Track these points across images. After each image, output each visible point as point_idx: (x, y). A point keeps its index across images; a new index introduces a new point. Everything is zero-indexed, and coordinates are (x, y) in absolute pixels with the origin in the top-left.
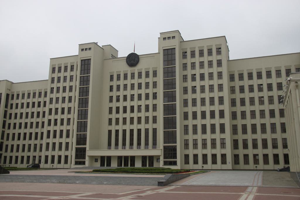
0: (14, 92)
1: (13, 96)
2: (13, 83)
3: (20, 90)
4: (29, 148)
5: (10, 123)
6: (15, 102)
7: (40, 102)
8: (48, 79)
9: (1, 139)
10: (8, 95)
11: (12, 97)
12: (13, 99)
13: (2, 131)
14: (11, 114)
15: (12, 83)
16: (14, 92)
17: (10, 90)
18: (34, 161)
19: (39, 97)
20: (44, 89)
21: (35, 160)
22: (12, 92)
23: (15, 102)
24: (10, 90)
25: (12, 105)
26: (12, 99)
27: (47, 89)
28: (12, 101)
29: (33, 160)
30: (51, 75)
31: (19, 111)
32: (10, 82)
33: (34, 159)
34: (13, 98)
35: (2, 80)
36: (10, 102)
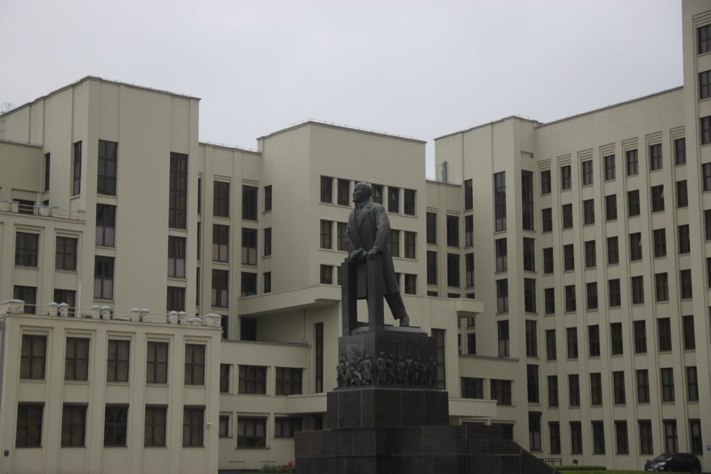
0: (549, 161)
1: (546, 175)
2: (540, 125)
3: (567, 148)
4: (639, 387)
5: (552, 290)
6: (556, 200)
7: (661, 187)
8: (681, 83)
9: (528, 354)
10: (526, 177)
11: (543, 183)
12: (549, 191)
13: (527, 321)
14: (548, 253)
15: (535, 125)
16: (549, 161)
17: (532, 155)
18: (670, 441)
19: (653, 168)
20: (671, 131)
21: (674, 437)
22: (540, 163)
23: (556, 200)
24: (532, 155)
25: (547, 213)
26: (543, 192)
27: (682, 128)
28: (547, 197)
29: (667, 437)
30: (696, 65)
31: (577, 236)
32: (530, 124)
33: (670, 433)
34: (547, 188)
35: (500, 119)
36: (540, 203)
